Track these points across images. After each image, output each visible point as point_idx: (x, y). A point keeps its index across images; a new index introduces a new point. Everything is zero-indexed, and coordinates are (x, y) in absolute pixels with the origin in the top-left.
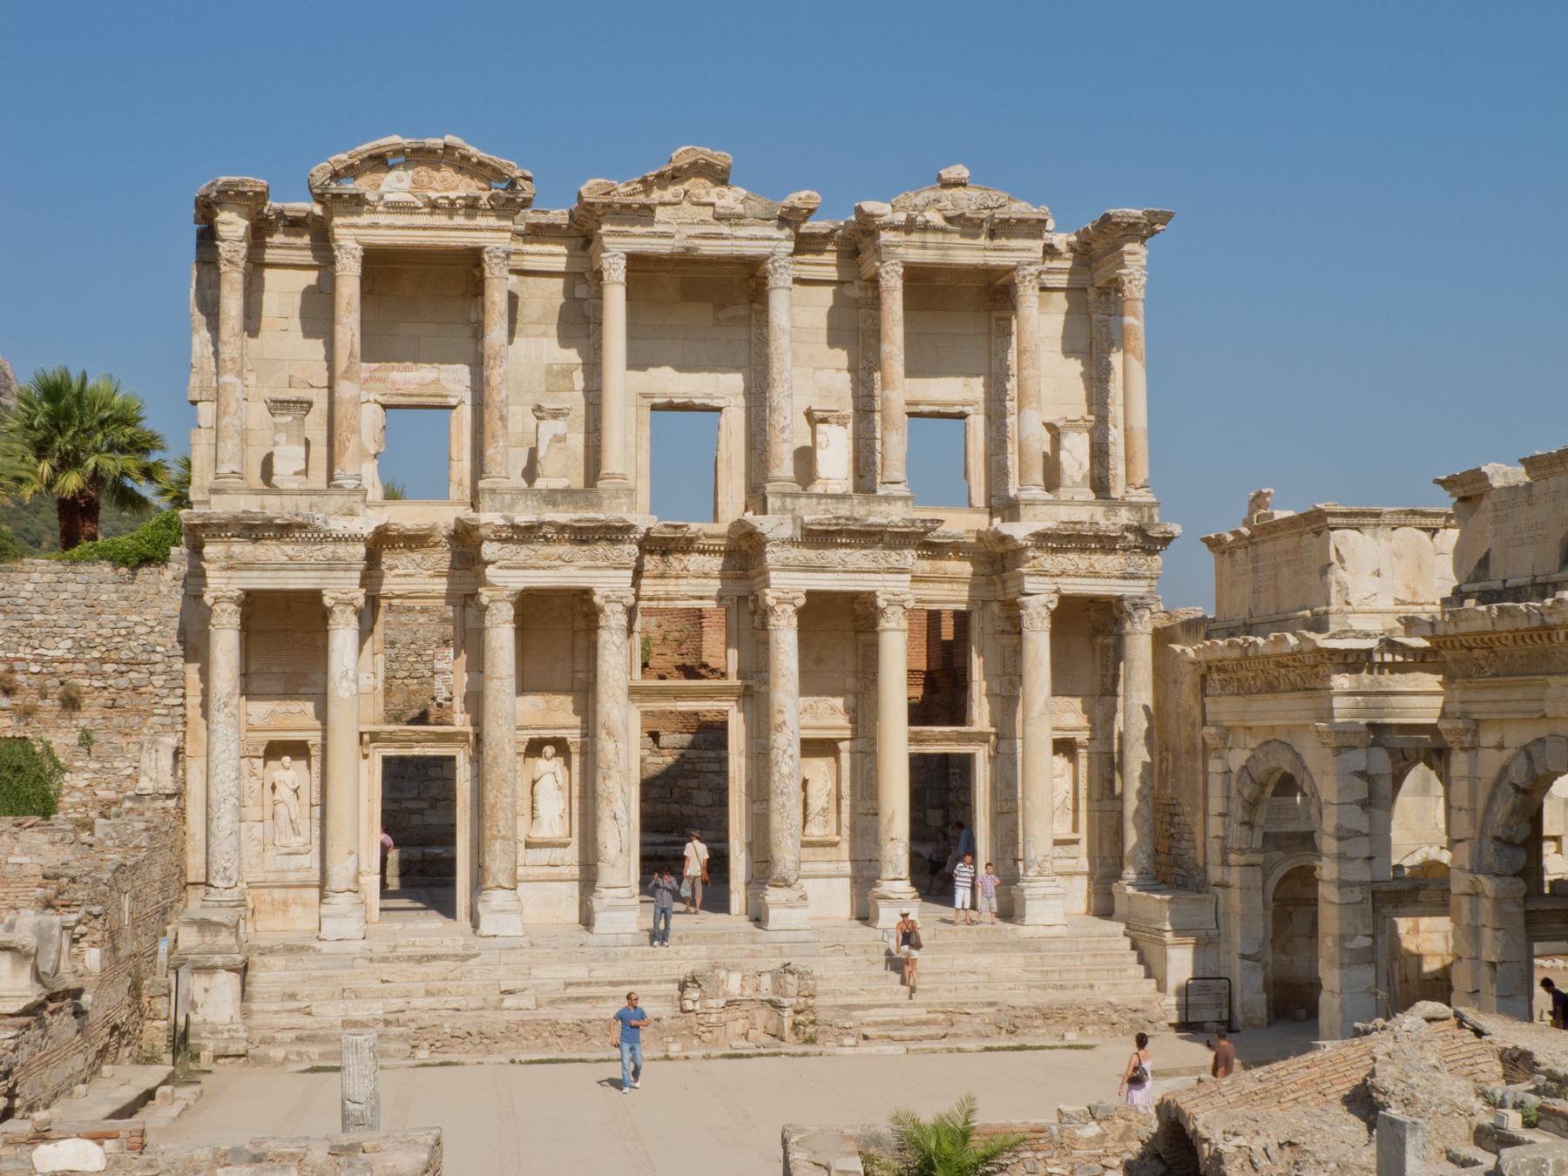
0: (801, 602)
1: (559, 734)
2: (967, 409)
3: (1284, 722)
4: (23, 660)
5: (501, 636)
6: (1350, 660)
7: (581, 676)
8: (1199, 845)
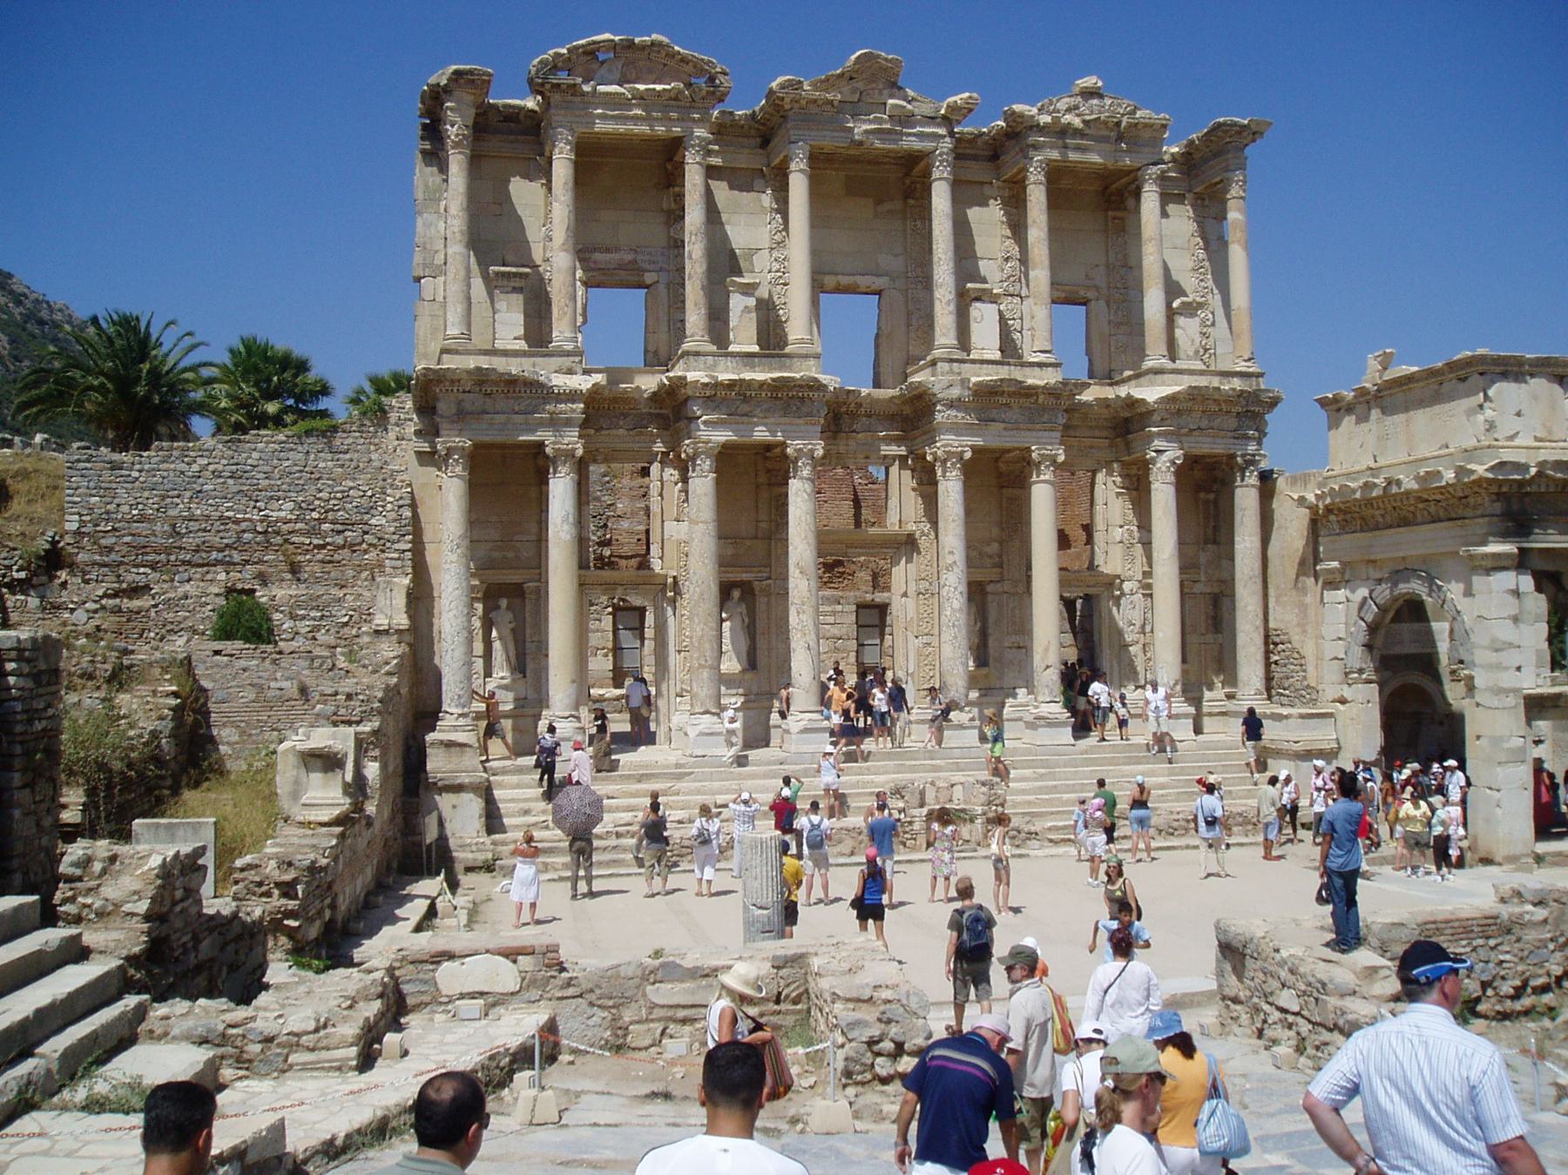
0: (968, 455)
1: (745, 576)
2: (1089, 295)
3: (1422, 551)
4: (250, 520)
5: (703, 483)
6: (1504, 489)
7: (764, 525)
8: (1310, 668)
